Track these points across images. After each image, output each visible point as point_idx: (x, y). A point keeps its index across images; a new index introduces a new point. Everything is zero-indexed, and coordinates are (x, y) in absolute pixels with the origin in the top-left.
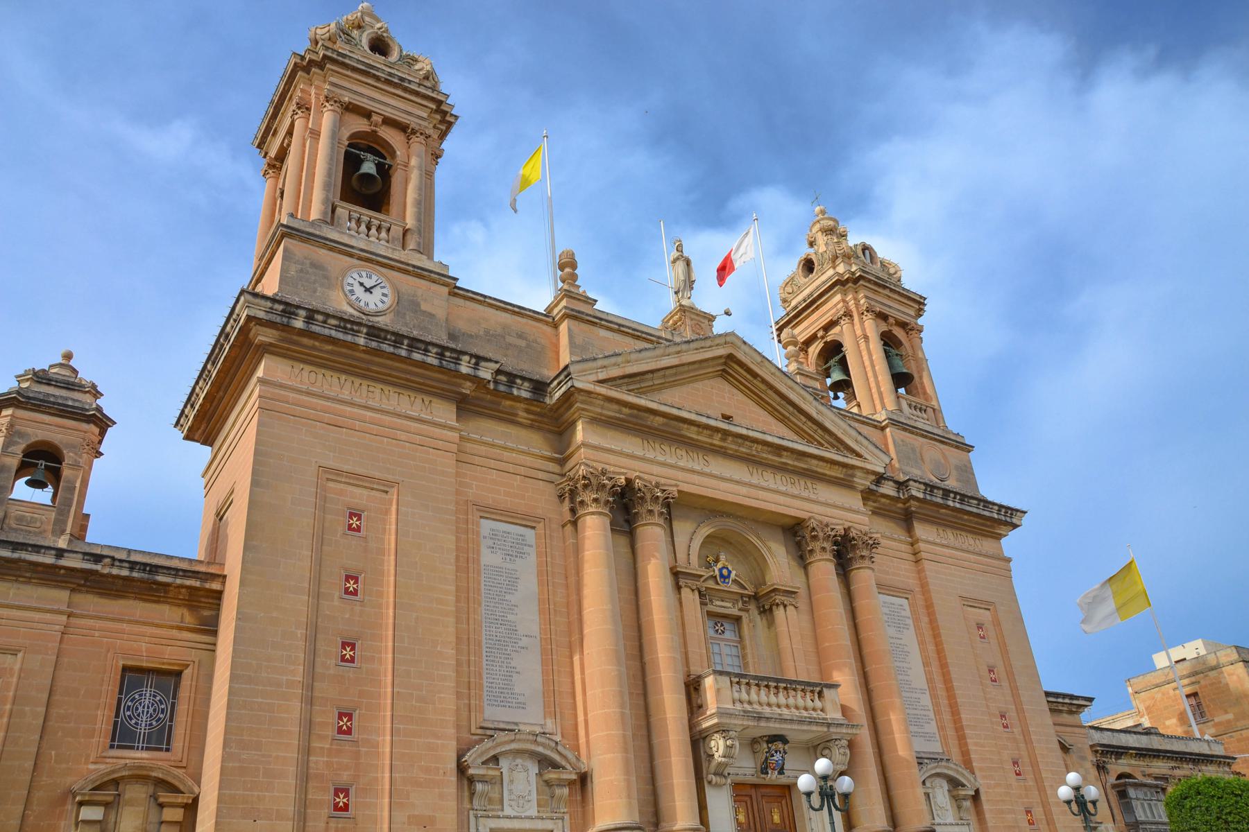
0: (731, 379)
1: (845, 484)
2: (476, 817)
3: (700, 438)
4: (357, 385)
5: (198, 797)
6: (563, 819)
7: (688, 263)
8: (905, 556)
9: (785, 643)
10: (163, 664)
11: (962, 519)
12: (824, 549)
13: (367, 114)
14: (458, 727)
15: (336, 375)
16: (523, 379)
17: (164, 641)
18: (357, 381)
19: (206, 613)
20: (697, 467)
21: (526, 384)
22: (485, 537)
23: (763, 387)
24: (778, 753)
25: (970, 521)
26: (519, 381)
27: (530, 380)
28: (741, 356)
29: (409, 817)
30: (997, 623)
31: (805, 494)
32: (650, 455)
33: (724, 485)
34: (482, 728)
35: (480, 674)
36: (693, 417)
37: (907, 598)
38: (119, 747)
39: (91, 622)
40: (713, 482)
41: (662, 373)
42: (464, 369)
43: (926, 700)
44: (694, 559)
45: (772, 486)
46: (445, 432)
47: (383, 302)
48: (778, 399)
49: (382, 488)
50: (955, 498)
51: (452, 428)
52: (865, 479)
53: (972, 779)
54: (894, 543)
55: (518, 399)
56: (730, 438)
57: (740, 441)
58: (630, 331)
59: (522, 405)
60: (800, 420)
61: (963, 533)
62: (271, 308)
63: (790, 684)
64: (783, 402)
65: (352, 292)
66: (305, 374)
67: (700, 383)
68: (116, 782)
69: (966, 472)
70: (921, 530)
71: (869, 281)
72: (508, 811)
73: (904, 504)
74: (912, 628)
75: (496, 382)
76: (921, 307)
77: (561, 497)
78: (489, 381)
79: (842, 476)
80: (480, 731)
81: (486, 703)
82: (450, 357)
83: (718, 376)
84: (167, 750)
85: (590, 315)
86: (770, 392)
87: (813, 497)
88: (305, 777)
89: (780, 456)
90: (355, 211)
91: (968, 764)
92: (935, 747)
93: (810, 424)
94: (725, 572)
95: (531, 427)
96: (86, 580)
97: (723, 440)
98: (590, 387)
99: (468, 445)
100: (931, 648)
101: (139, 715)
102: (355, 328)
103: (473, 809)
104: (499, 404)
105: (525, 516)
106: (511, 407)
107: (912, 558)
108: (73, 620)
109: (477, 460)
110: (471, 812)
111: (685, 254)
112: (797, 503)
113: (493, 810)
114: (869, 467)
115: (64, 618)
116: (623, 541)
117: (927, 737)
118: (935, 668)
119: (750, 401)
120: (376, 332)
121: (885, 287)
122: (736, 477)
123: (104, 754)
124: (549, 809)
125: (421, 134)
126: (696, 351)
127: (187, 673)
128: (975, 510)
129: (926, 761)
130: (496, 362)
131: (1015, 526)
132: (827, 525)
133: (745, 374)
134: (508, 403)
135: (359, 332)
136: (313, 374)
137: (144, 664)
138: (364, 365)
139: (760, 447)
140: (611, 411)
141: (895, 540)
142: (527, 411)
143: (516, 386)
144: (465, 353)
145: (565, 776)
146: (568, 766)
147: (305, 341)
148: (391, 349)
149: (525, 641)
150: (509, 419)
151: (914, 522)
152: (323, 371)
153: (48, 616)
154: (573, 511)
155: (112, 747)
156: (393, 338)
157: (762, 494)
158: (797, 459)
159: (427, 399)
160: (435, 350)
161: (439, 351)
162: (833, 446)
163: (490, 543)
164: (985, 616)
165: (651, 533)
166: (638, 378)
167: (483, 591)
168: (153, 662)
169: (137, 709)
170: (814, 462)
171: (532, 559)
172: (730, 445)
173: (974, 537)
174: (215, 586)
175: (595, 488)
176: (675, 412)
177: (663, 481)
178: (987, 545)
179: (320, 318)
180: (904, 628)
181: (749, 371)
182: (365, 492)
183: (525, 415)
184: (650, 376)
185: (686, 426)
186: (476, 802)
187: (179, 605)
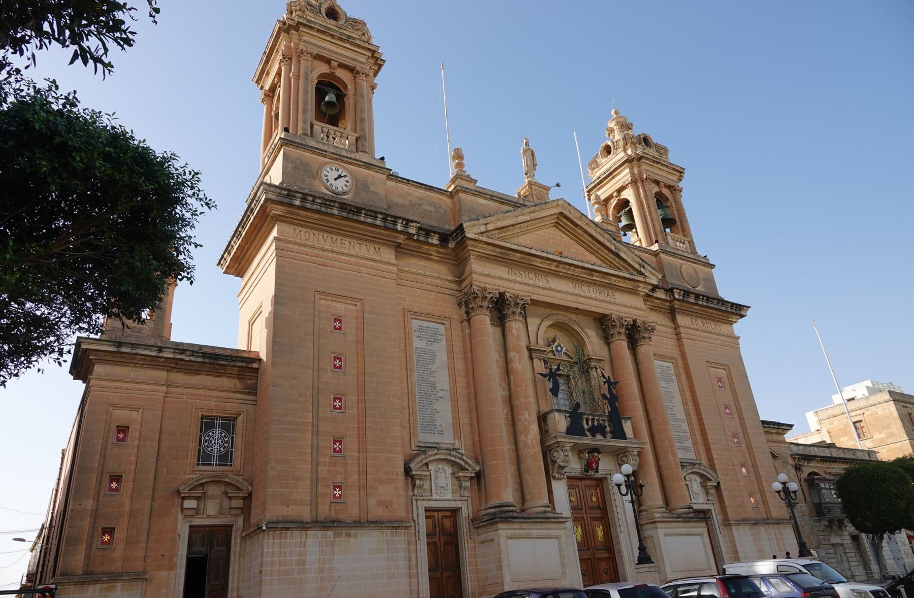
1: (633, 292)
2: (416, 500)
3: (543, 266)
4: (334, 239)
5: (251, 492)
6: (467, 500)
7: (533, 154)
8: (670, 336)
10: (226, 414)
11: (708, 312)
12: (620, 333)
13: (328, 61)
14: (403, 446)
15: (321, 234)
17: (225, 400)
18: (334, 237)
19: (249, 382)
20: (541, 284)
22: (415, 331)
23: (581, 232)
28: (567, 213)
29: (378, 501)
31: (608, 299)
32: (513, 277)
33: (558, 295)
34: (417, 446)
35: (416, 414)
36: (538, 253)
37: (672, 363)
38: (202, 464)
39: (181, 390)
40: (553, 293)
41: (519, 225)
43: (685, 426)
44: (541, 342)
45: (588, 295)
46: (389, 267)
47: (346, 186)
48: (591, 239)
50: (703, 299)
51: (393, 265)
52: (646, 288)
53: (715, 476)
55: (432, 245)
56: (562, 265)
57: (567, 267)
58: (498, 199)
59: (435, 248)
61: (709, 321)
62: (280, 193)
64: (594, 242)
65: (327, 180)
66: (303, 233)
68: (202, 485)
69: (710, 281)
70: (681, 320)
71: (648, 159)
72: (435, 496)
73: (670, 303)
74: (676, 381)
75: (418, 235)
76: (682, 174)
77: (460, 305)
78: (414, 235)
79: (631, 287)
80: (416, 449)
81: (419, 431)
82: (391, 221)
83: (553, 226)
84: (231, 465)
85: (473, 190)
87: (612, 300)
88: (316, 480)
89: (592, 275)
90: (325, 127)
91: (712, 466)
92: (691, 456)
94: (559, 348)
95: (440, 262)
96: (177, 364)
99: (403, 274)
100: (688, 394)
101: (212, 445)
102: (332, 204)
103: (414, 496)
104: (420, 248)
106: (428, 250)
107: (675, 337)
108: (170, 389)
110: (413, 497)
111: (531, 147)
112: (604, 305)
113: (426, 496)
115: (165, 388)
116: (498, 330)
117: (687, 450)
118: (691, 406)
119: (573, 242)
120: (345, 207)
121: (658, 163)
122: (564, 290)
123: (194, 469)
124: (459, 495)
125: (363, 74)
127: (240, 419)
128: (716, 307)
129: (686, 464)
130: (419, 223)
131: (742, 316)
132: (622, 318)
133: (570, 224)
134: (426, 247)
135: (334, 206)
136: (307, 234)
137: (214, 414)
139: (580, 270)
140: (489, 250)
141: (664, 326)
142: (438, 252)
144: (400, 218)
145: (468, 475)
146: (470, 469)
147: (302, 212)
149: (441, 394)
150: (427, 257)
151: (677, 316)
152: (313, 231)
153: (155, 387)
154: (467, 313)
155: (198, 464)
157: (581, 300)
161: (384, 216)
162: (626, 269)
163: (418, 334)
164: (722, 373)
165: (515, 326)
166: (504, 230)
167: (415, 363)
168: (219, 413)
169: (211, 441)
174: (255, 365)
175: (481, 299)
176: (527, 250)
177: (521, 293)
178: (724, 328)
179: (310, 198)
181: (572, 222)
184: (512, 228)
185: (534, 259)
186: (416, 492)
187: (232, 378)
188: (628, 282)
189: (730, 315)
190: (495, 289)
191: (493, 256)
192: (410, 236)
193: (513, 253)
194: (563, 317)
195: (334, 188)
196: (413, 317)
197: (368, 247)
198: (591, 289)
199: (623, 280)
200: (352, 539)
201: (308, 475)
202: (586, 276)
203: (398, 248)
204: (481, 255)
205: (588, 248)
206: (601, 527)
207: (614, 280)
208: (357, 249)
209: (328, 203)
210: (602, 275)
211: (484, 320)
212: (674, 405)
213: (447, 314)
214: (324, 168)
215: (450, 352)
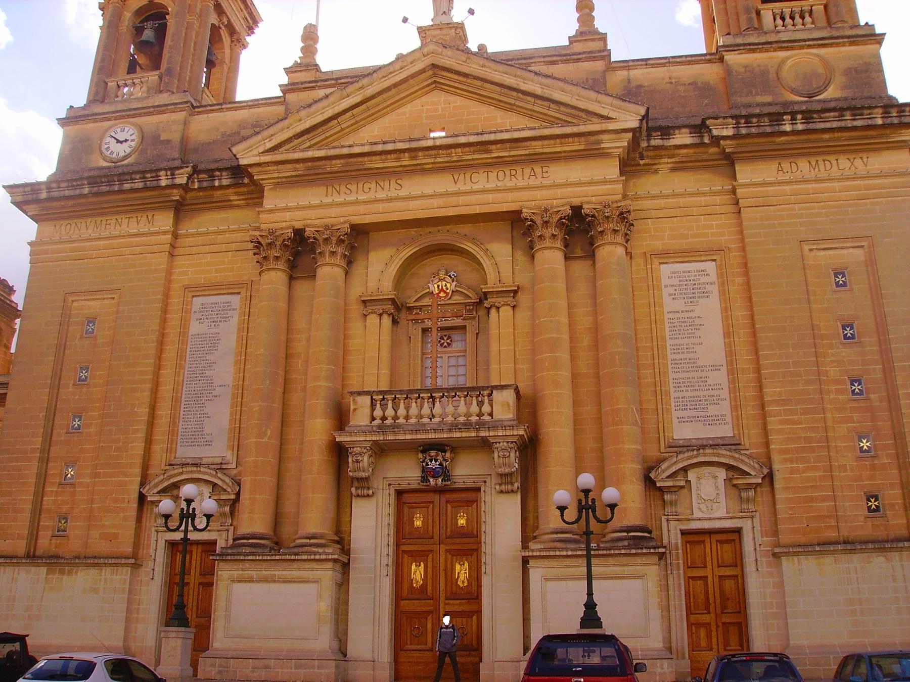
0: (446, 87)
3: (386, 165)
15: (83, 221)
16: (220, 170)
18: (99, 219)
21: (224, 174)
22: (195, 312)
23: (479, 83)
24: (433, 461)
25: (837, 139)
26: (218, 173)
27: (226, 169)
30: (871, 262)
31: (533, 182)
33: (412, 204)
34: (170, 465)
36: (366, 149)
41: (349, 114)
42: (163, 183)
43: (721, 377)
48: (498, 89)
49: (110, 296)
50: (793, 119)
54: (703, 198)
55: (221, 187)
56: (420, 154)
57: (433, 152)
59: (231, 191)
60: (528, 102)
61: (832, 158)
63: (448, 392)
67: (409, 106)
79: (582, 147)
86: (487, 85)
87: (546, 182)
88: (37, 511)
92: (725, 431)
93: (539, 102)
95: (248, 205)
97: (412, 158)
98: (256, 160)
100: (740, 314)
105: (231, 285)
107: (731, 208)
109: (194, 250)
114: (612, 126)
118: (742, 337)
124: (219, 524)
126: (384, 79)
128: (835, 125)
132: (546, 210)
133: (456, 77)
136: (69, 226)
138: (97, 206)
140: (287, 171)
141: (704, 194)
142: (237, 194)
143: (216, 178)
146: (229, 490)
148: (108, 189)
150: (226, 205)
152: (75, 221)
156: (106, 180)
157: (462, 199)
158: (511, 149)
159: (150, 215)
160: (138, 177)
162: (579, 118)
163: (199, 315)
166: (320, 130)
170: (534, 143)
172: (422, 159)
173: (851, 156)
180: (699, 297)
182: (99, 302)
183: (236, 198)
184: (334, 122)
185: (366, 159)
188: (571, 140)
189: (888, 132)
190: (287, 228)
191: (296, 176)
193: (328, 162)
195: (114, 155)
196: (194, 294)
197: (139, 219)
198: (493, 175)
199: (576, 139)
200: (65, 577)
201: (29, 507)
202: (476, 156)
204: (280, 180)
205: (498, 104)
206: (466, 565)
207: (538, 147)
208: (124, 226)
209: (75, 183)
210: (508, 145)
212: (699, 341)
213: (246, 278)
214: (108, 135)
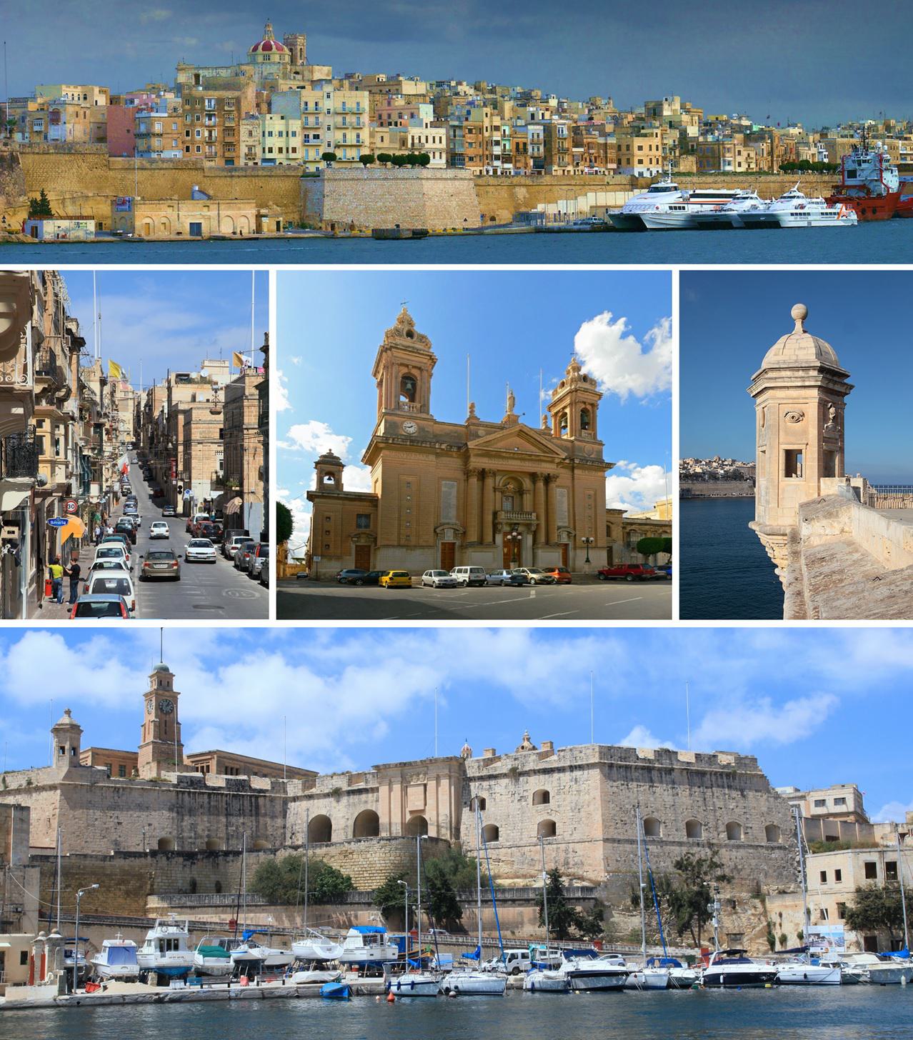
1: (552, 462)
9: (525, 503)
30: (595, 494)
91: (575, 529)
100: (571, 501)
116: (480, 483)
118: (571, 506)
140: (480, 452)
171: (455, 489)
192: (443, 449)
194: (513, 475)
203: (437, 455)
207: (542, 458)
211: (474, 481)
215: (458, 491)
